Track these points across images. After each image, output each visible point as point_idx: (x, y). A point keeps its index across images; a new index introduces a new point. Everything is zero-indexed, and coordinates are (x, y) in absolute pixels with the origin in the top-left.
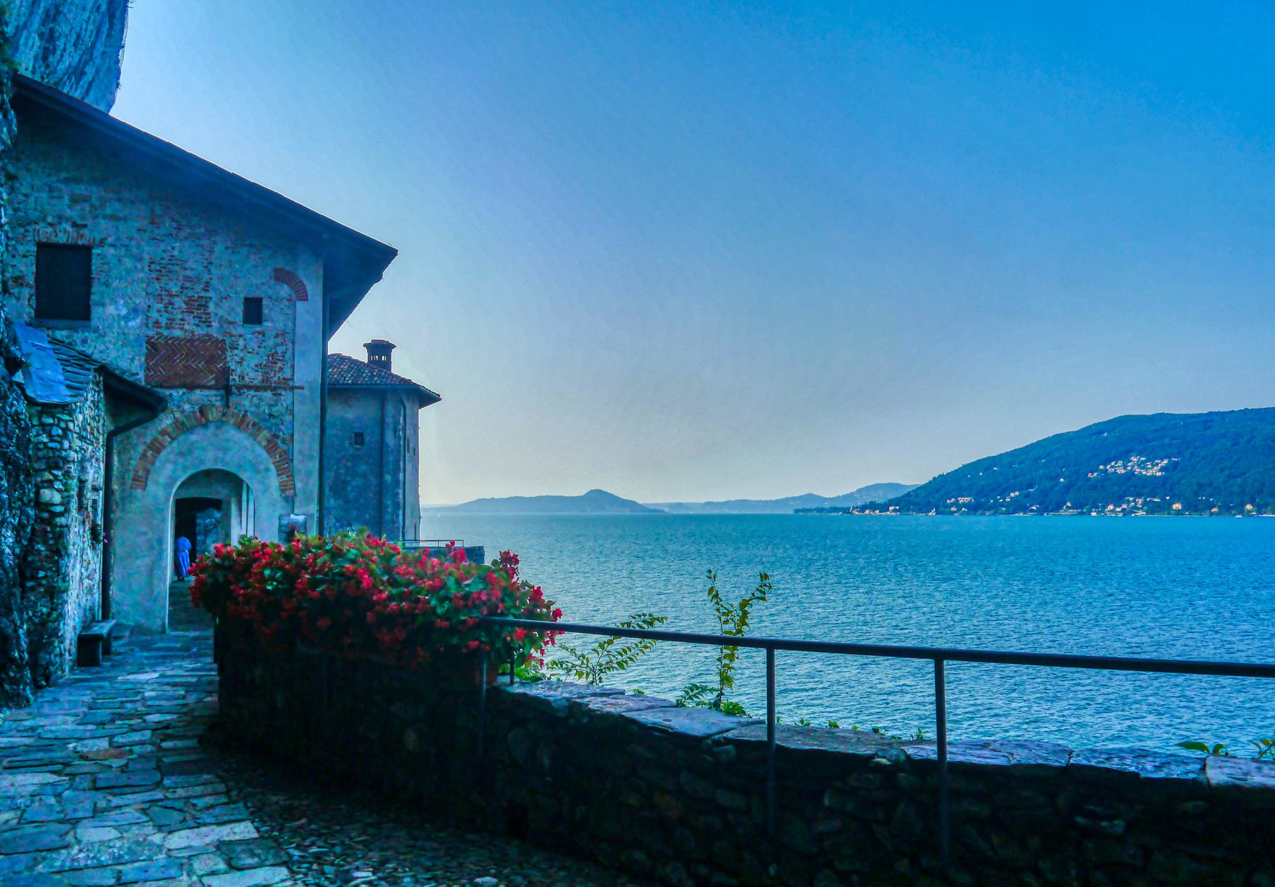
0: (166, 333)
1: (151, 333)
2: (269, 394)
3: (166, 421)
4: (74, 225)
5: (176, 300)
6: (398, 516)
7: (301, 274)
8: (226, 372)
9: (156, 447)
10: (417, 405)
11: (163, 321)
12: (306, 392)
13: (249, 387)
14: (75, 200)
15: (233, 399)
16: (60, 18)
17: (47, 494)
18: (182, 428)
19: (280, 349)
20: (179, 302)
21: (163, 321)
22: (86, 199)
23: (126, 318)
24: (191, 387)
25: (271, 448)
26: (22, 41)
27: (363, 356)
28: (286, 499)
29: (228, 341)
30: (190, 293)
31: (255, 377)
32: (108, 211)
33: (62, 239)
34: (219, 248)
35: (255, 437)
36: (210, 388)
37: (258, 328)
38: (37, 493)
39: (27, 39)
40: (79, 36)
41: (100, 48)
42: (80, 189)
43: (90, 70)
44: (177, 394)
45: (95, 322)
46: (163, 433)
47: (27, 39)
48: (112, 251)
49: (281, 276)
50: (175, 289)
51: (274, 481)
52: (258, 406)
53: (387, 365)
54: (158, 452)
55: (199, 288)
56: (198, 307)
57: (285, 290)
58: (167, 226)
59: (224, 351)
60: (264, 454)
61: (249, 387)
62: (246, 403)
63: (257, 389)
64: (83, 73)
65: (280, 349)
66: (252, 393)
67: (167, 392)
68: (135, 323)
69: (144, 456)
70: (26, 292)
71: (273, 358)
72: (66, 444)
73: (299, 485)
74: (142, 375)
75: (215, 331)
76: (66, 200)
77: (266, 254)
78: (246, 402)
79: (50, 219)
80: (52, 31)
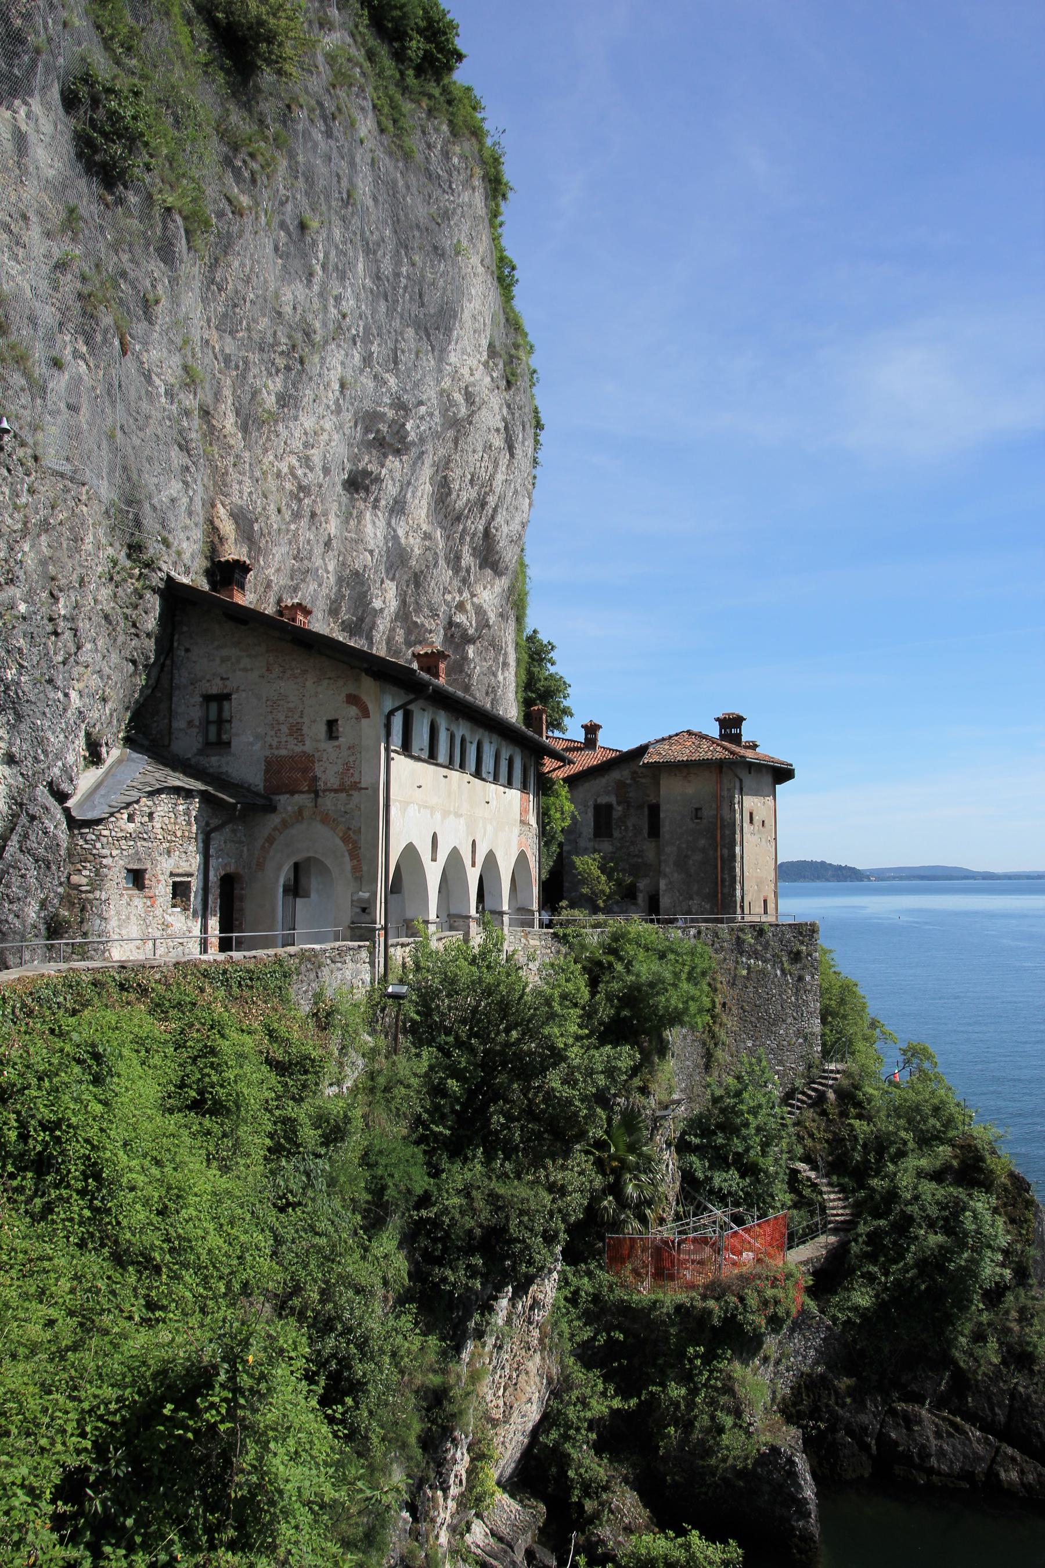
0: (276, 752)
1: (268, 753)
2: (344, 795)
3: (275, 820)
4: (222, 679)
5: (282, 727)
6: (735, 889)
7: (364, 698)
8: (315, 779)
9: (271, 840)
10: (768, 779)
11: (274, 744)
12: (369, 792)
13: (330, 790)
14: (224, 660)
15: (320, 800)
16: (452, 465)
17: (75, 879)
18: (285, 824)
19: (351, 759)
20: (284, 729)
21: (274, 744)
22: (228, 658)
23: (252, 744)
24: (292, 793)
25: (345, 839)
26: (409, 495)
27: (714, 731)
28: (356, 879)
29: (317, 755)
30: (291, 720)
31: (334, 782)
32: (242, 666)
33: (214, 691)
34: (309, 684)
35: (334, 830)
36: (302, 792)
37: (336, 743)
38: (68, 878)
39: (413, 493)
40: (473, 476)
41: (500, 477)
42: (225, 652)
43: (492, 500)
44: (283, 798)
45: (233, 749)
46: (275, 829)
47: (413, 493)
48: (244, 695)
49: (353, 700)
50: (282, 718)
51: (348, 864)
52: (336, 805)
53: (736, 739)
54: (271, 844)
55: (296, 716)
56: (296, 731)
57: (353, 711)
58: (277, 670)
59: (313, 762)
60: (341, 844)
61: (330, 790)
62: (328, 803)
63: (336, 791)
64: (483, 504)
65: (351, 759)
66: (333, 794)
67: (277, 798)
68: (257, 747)
69: (263, 847)
70: (196, 730)
71: (347, 767)
72: (98, 845)
73: (365, 868)
74: (261, 786)
75: (308, 747)
76: (218, 661)
77: (341, 682)
78: (328, 802)
79: (208, 677)
80: (445, 477)
